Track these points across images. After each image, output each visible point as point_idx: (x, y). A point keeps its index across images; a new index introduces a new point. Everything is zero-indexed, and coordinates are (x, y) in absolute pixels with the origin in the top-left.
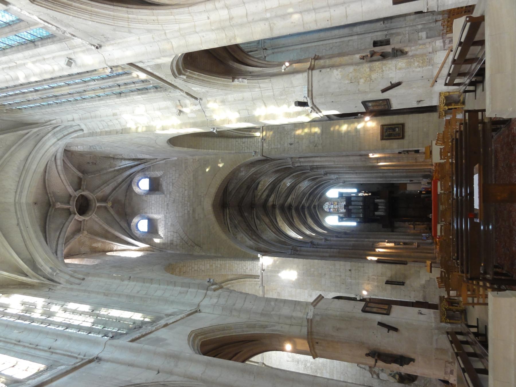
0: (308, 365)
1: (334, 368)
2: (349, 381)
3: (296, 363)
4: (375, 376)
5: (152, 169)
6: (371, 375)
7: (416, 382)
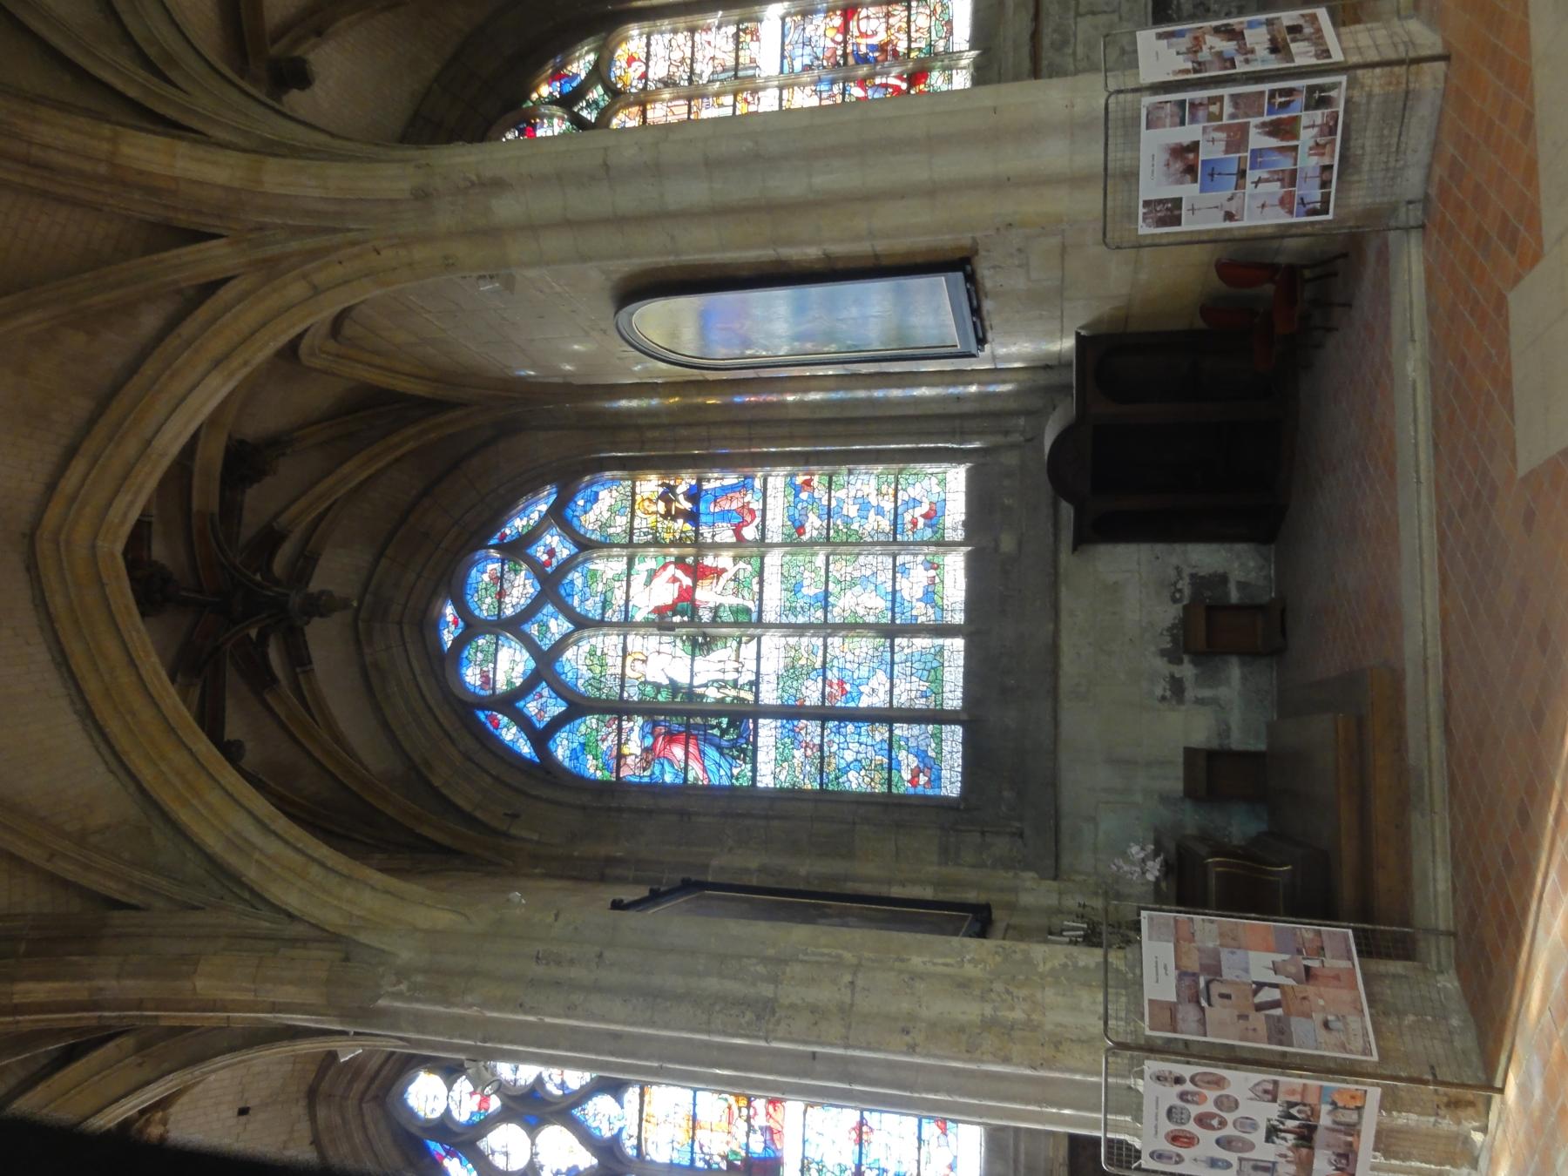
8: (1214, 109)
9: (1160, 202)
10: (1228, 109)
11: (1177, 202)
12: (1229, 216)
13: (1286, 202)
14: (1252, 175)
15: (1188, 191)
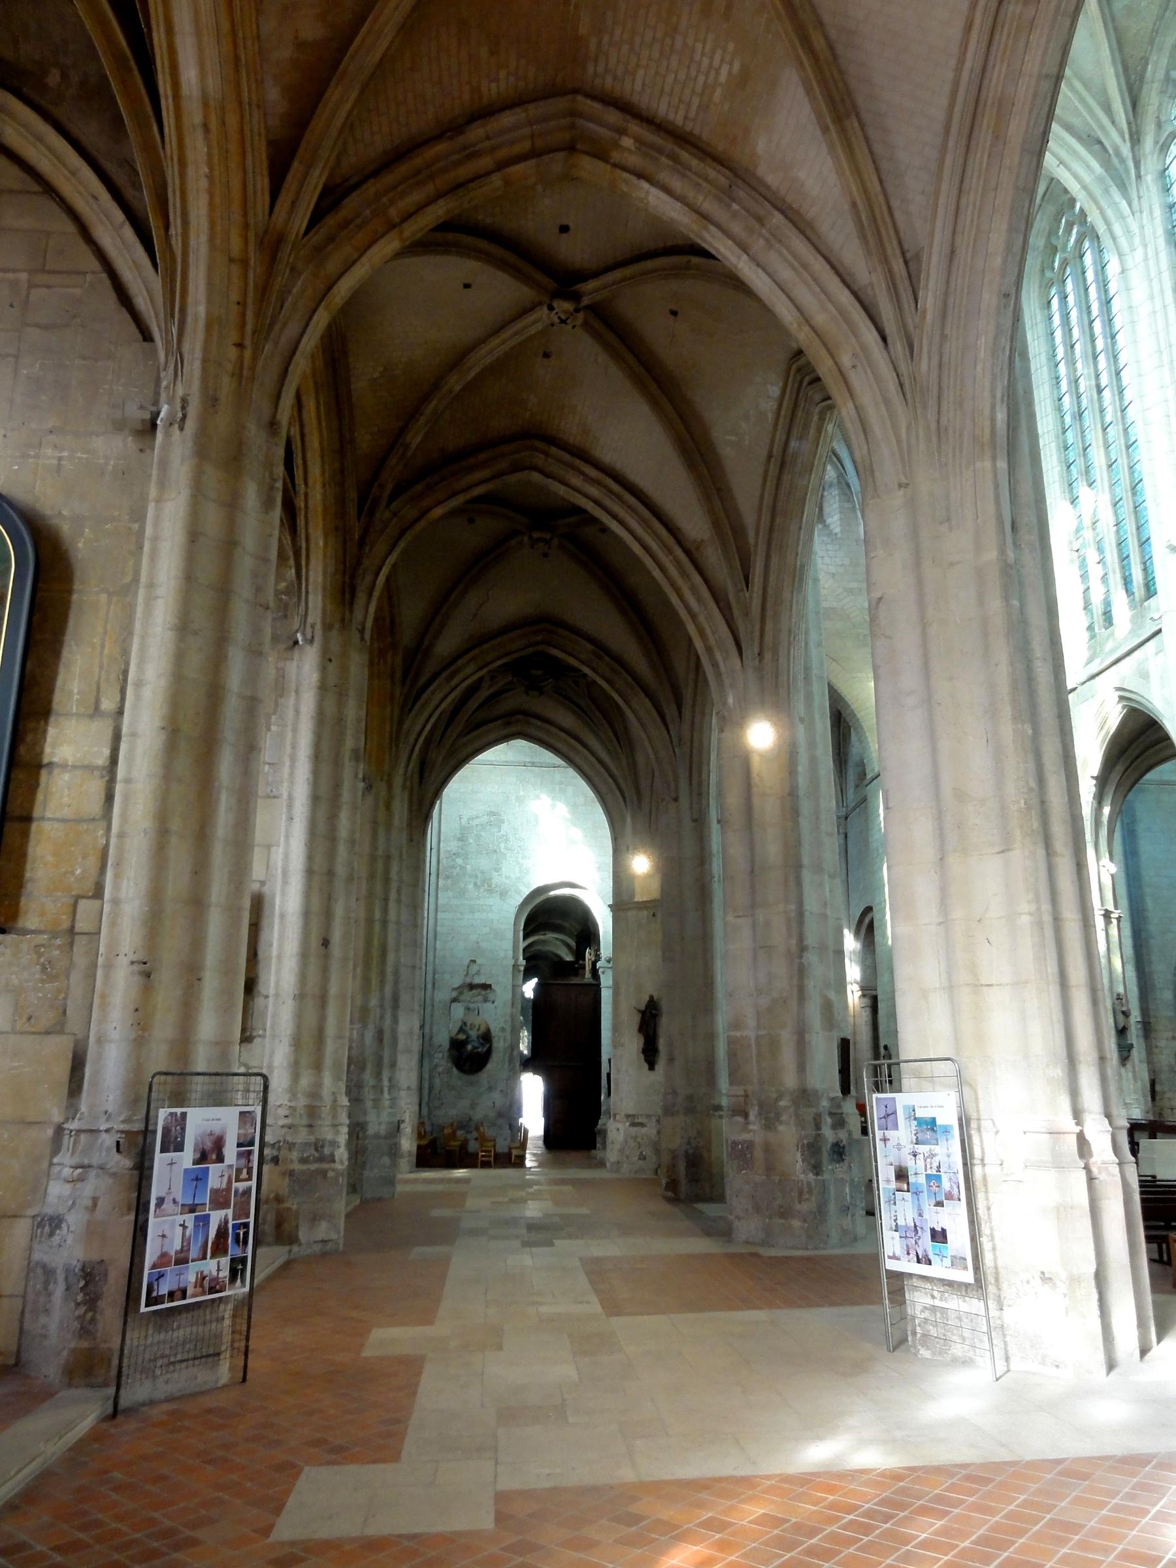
0: (459, 861)
1: (462, 914)
3: (458, 835)
4: (454, 994)
5: (847, 505)
8: (244, 1175)
9: (183, 1129)
10: (242, 1186)
11: (179, 1148)
12: (161, 1201)
13: (163, 1260)
14: (189, 1219)
15: (186, 1158)
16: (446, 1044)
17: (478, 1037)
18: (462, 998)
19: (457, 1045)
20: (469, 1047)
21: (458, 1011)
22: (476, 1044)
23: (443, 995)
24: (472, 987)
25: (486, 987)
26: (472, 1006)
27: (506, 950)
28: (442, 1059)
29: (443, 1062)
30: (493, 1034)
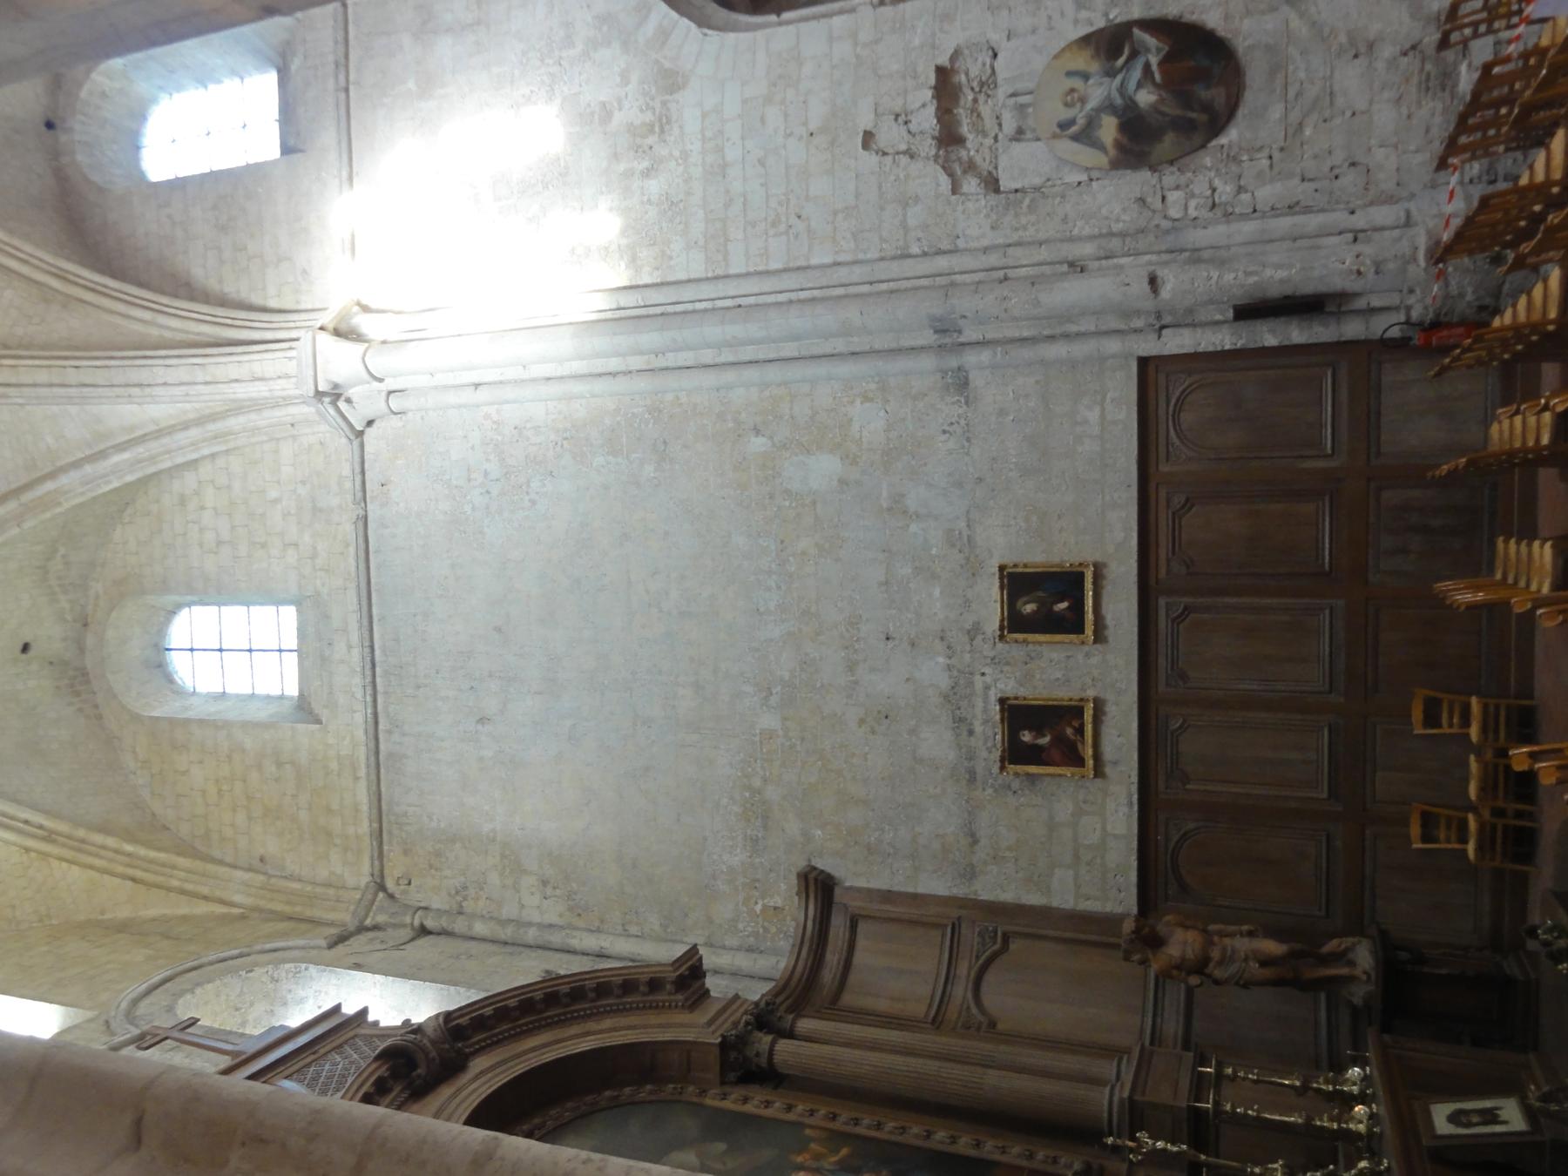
1: (727, 206)
2: (814, 261)
4: (971, 185)
6: (945, 181)
7: (1231, 136)
16: (1138, 181)
17: (1111, 73)
18: (985, 166)
19: (1138, 142)
20: (1146, 98)
21: (1022, 164)
22: (1136, 73)
23: (975, 220)
24: (949, 138)
25: (945, 85)
26: (1009, 125)
27: (831, 39)
28: (1188, 188)
29: (1200, 186)
30: (1100, 23)
